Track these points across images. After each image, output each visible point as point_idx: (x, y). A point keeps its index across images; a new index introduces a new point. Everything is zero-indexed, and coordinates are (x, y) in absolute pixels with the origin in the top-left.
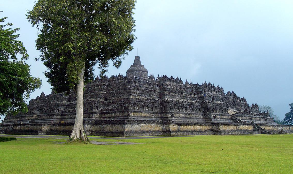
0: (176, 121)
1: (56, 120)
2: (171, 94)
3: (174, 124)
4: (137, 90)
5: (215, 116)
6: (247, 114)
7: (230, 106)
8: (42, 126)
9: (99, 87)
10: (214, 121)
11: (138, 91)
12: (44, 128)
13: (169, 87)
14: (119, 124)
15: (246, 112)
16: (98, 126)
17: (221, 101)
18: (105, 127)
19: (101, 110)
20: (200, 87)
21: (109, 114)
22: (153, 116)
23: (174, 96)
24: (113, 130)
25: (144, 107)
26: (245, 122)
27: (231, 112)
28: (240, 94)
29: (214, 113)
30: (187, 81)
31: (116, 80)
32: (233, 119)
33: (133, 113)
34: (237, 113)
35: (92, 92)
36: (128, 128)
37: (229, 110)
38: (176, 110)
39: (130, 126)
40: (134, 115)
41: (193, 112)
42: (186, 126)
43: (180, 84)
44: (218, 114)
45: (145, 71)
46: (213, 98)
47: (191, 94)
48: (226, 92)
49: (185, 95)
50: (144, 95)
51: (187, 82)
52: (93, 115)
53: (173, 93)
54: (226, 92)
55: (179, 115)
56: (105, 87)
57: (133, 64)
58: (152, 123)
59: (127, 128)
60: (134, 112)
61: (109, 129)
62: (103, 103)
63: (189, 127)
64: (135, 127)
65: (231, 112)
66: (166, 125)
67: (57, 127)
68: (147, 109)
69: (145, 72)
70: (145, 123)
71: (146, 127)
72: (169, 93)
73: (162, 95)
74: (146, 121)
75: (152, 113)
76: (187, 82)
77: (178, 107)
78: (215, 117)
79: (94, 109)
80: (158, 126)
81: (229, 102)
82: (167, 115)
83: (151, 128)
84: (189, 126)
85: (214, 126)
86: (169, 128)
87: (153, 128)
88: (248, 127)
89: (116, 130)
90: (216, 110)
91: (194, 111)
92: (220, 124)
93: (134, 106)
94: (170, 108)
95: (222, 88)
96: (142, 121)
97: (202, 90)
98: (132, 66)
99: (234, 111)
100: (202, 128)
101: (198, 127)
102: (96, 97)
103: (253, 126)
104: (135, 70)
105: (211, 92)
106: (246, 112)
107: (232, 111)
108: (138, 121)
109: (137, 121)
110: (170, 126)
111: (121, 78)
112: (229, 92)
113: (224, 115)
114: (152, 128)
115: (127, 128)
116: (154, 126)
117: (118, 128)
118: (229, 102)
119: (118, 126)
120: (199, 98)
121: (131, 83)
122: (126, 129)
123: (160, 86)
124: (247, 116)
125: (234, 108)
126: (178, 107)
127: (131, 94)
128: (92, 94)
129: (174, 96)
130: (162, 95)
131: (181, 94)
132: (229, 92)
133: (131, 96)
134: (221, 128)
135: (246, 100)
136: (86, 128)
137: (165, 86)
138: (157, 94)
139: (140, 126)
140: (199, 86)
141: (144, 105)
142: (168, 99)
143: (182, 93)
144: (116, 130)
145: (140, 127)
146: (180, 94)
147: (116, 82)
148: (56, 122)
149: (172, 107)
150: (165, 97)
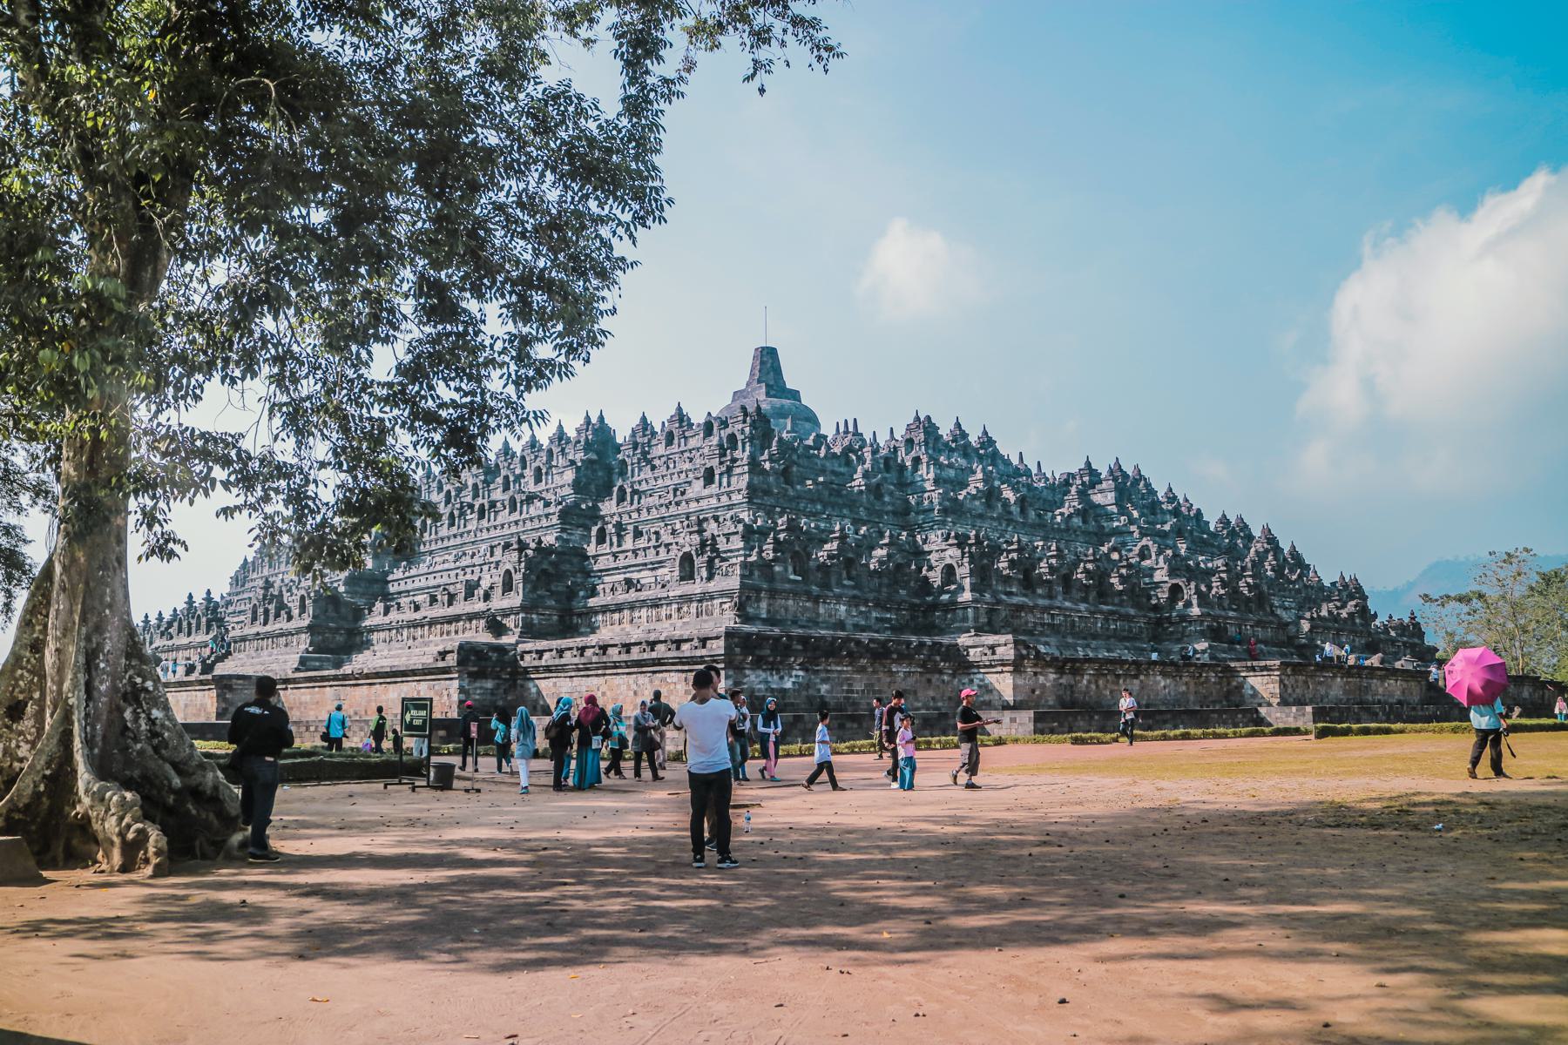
3: (1035, 665)
23: (981, 516)
33: (764, 605)
40: (769, 612)
57: (743, 387)
63: (1118, 683)
64: (788, 685)
88: (1405, 685)
100: (1184, 688)
101: (1162, 684)
112: (1224, 521)
129: (981, 516)
132: (1224, 521)
134: (1290, 690)
138: (889, 508)
139: (823, 675)
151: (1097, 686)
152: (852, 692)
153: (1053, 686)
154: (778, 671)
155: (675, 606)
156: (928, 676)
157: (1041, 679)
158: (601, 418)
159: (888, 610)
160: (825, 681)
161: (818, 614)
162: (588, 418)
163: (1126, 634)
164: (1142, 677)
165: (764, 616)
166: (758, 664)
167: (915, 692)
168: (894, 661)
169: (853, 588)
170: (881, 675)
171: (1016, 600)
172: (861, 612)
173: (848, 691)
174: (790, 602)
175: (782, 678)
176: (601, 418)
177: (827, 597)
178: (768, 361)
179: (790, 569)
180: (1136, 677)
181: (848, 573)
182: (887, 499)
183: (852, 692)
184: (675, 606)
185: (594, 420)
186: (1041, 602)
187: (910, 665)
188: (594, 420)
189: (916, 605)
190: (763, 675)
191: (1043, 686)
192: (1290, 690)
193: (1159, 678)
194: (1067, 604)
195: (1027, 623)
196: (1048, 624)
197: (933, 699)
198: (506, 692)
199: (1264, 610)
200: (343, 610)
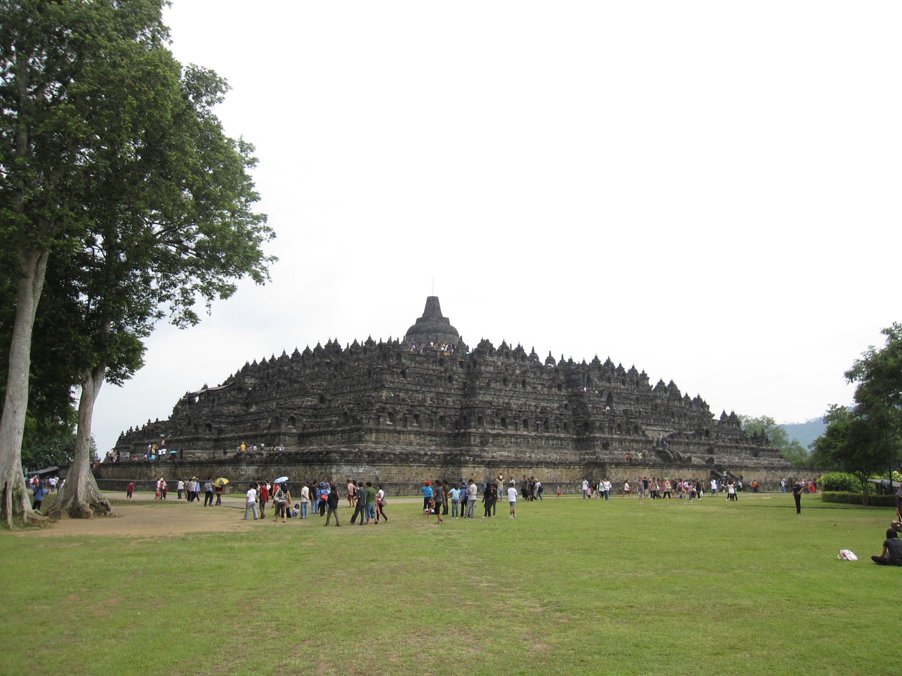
0: (495, 454)
1: (199, 453)
2: (493, 385)
3: (474, 464)
4: (401, 375)
5: (605, 442)
6: (701, 439)
7: (654, 417)
8: (150, 467)
9: (316, 369)
10: (601, 456)
11: (402, 379)
12: (155, 471)
13: (492, 369)
14: (319, 462)
15: (699, 433)
16: (276, 468)
17: (631, 405)
18: (290, 471)
19: (304, 427)
20: (576, 368)
21: (319, 438)
22: (432, 441)
24: (305, 479)
25: (406, 418)
26: (690, 458)
27: (656, 433)
28: (688, 389)
29: (602, 436)
30: (533, 350)
31: (360, 353)
32: (658, 452)
33: (374, 435)
34: (672, 436)
35: (295, 382)
36: (340, 473)
37: (652, 428)
38: (496, 427)
39: (346, 469)
40: (376, 438)
41: (548, 432)
42: (510, 470)
43: (525, 362)
44: (615, 436)
45: (451, 333)
46: (610, 396)
47: (550, 387)
48: (653, 382)
49: (534, 388)
50: (418, 388)
51: (550, 359)
52: (282, 440)
53: (498, 384)
54: (653, 382)
55: (504, 440)
56: (332, 368)
58: (414, 461)
59: (335, 473)
60: (378, 431)
61: (299, 475)
62: (314, 408)
63: (520, 471)
64: (361, 470)
65: (656, 433)
66: (454, 464)
67: (188, 471)
68: (415, 424)
69: (451, 335)
70: (391, 461)
71: (394, 470)
72: (488, 385)
73: (468, 391)
74: (394, 454)
75: (429, 435)
76: (550, 359)
77: (503, 420)
78: (605, 446)
79: (283, 426)
80: (432, 469)
81: (655, 407)
82: (470, 441)
83: (412, 474)
84: (522, 470)
85: (594, 468)
86: (459, 474)
87: (416, 474)
88: (695, 472)
89: (312, 478)
90: (611, 428)
91: (550, 430)
92: (611, 464)
93: (379, 416)
94: (480, 420)
95: (643, 372)
96: (383, 455)
97: (581, 376)
98: (418, 320)
99: (667, 429)
101: (547, 471)
102: (303, 395)
103: (709, 471)
104: (425, 328)
105: (610, 383)
106: (699, 433)
107: (660, 429)
108: (369, 454)
109: (366, 456)
110: (464, 470)
111: (371, 346)
112: (661, 383)
113: (633, 441)
114: (414, 474)
115: (335, 473)
116: (420, 469)
117: (316, 473)
118: (655, 407)
119: (317, 468)
120: (569, 398)
121: (389, 358)
122: (334, 476)
123: (469, 367)
124: (700, 444)
125: (665, 422)
126: (503, 420)
127: (383, 386)
128: (296, 386)
130: (468, 391)
131: (521, 386)
132: (661, 383)
133: (382, 390)
134: (614, 475)
135: (707, 404)
136: (243, 473)
137: (480, 365)
138: (456, 386)
139: (377, 467)
140: (573, 368)
141: (409, 414)
142: (484, 397)
143: (524, 384)
144: (312, 478)
145: (377, 472)
146: (519, 386)
147: (361, 356)
148: (199, 458)
149: (484, 418)
150: (476, 394)
151: (508, 473)
152: (391, 474)
153: (484, 472)
154: (356, 465)
155: (340, 435)
156: (429, 468)
157: (477, 469)
158: (336, 341)
159: (436, 436)
160: (377, 469)
161: (400, 439)
162: (330, 341)
163: (559, 446)
164: (534, 469)
165: (374, 440)
166: (348, 462)
167: (422, 474)
168: (411, 462)
169: (418, 427)
170: (405, 467)
171: (495, 432)
172: (421, 438)
173: (389, 474)
174: (387, 434)
175: (358, 468)
176: (336, 341)
177: (404, 431)
178: (433, 304)
179: (388, 419)
180: (531, 468)
181: (417, 421)
182: (454, 382)
183: (391, 474)
184: (340, 435)
185: (333, 342)
186: (509, 432)
187: (419, 463)
188: (333, 342)
189: (449, 434)
190: (349, 467)
191: (478, 472)
192: (614, 475)
193: (544, 469)
194: (525, 433)
195: (501, 442)
196: (514, 442)
197: (431, 477)
198: (262, 471)
199: (638, 434)
200: (213, 430)
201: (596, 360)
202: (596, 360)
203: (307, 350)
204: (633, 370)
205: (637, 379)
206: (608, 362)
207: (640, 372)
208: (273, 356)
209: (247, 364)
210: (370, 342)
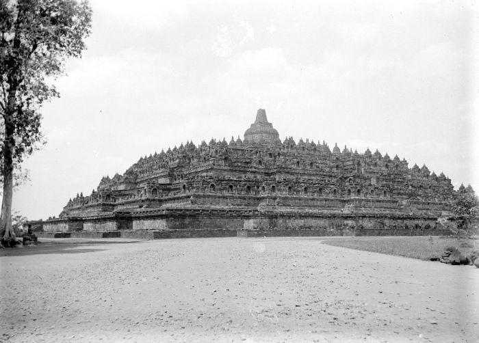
28: (436, 169)
48: (410, 166)
54: (410, 166)
112: (416, 167)
132: (416, 167)
158: (192, 143)
162: (188, 143)
178: (262, 114)
201: (368, 152)
202: (368, 152)
203: (175, 149)
204: (397, 158)
205: (399, 164)
206: (377, 153)
207: (401, 159)
208: (156, 153)
209: (141, 159)
210: (213, 142)
